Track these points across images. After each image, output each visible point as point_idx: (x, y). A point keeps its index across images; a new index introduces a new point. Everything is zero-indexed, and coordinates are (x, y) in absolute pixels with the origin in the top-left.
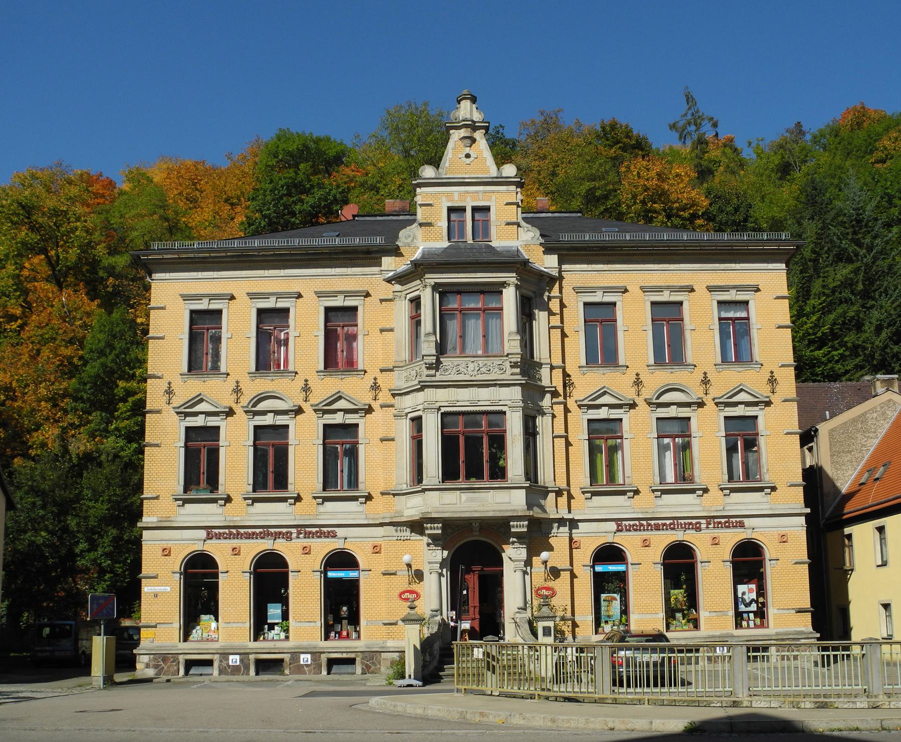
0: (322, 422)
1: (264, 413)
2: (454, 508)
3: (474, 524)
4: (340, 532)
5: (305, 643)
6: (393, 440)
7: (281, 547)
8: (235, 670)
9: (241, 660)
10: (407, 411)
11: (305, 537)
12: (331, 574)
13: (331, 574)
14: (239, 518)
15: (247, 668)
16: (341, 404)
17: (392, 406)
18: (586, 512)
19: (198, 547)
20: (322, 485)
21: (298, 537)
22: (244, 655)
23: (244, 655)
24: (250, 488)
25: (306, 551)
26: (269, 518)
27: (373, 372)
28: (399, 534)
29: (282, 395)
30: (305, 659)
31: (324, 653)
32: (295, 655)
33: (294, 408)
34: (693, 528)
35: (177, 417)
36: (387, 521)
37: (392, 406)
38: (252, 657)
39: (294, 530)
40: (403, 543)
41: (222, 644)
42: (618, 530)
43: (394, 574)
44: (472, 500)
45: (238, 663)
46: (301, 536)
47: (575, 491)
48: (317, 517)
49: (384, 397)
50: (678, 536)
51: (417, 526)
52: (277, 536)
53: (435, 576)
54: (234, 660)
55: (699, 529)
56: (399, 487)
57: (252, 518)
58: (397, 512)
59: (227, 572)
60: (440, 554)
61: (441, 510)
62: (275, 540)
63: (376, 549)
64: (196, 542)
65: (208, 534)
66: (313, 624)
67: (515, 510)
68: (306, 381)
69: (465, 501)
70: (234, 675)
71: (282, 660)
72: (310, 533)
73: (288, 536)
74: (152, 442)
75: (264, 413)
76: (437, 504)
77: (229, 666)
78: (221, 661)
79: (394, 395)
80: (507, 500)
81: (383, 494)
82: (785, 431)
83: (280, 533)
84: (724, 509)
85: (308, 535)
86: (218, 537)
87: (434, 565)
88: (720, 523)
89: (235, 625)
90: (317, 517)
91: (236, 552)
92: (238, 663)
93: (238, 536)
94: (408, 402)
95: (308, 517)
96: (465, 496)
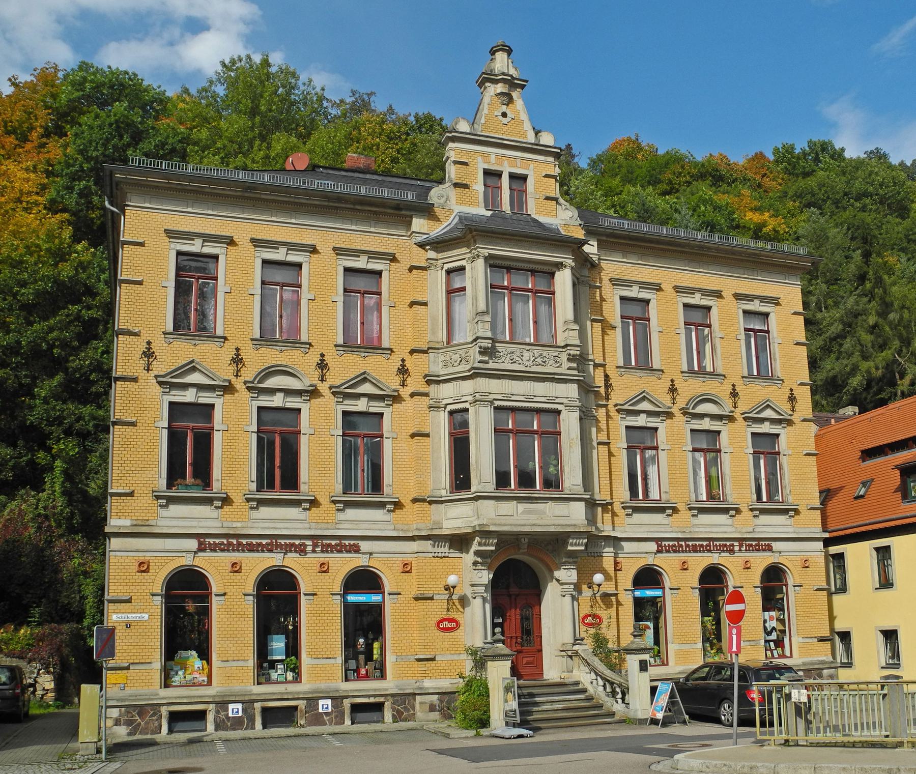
0: (341, 408)
1: (272, 391)
2: (510, 520)
3: (523, 540)
4: (364, 546)
5: (323, 685)
6: (427, 435)
7: (292, 562)
8: (237, 723)
9: (244, 710)
10: (445, 402)
11: (322, 551)
12: (352, 598)
13: (352, 598)
14: (239, 525)
15: (252, 720)
16: (367, 388)
17: (427, 395)
18: (627, 529)
19: (187, 561)
20: (341, 486)
21: (314, 551)
22: (247, 704)
23: (247, 704)
24: (254, 486)
25: (324, 569)
26: (278, 525)
27: (402, 352)
28: (436, 549)
29: (298, 371)
30: (325, 705)
31: (347, 697)
32: (312, 701)
33: (310, 388)
34: (727, 550)
35: (158, 389)
36: (423, 533)
37: (427, 395)
38: (258, 706)
39: (309, 543)
40: (440, 561)
41: (218, 689)
42: (659, 551)
43: (431, 599)
44: (529, 512)
45: (240, 714)
46: (318, 549)
47: (617, 507)
48: (337, 526)
49: (415, 383)
50: (714, 558)
51: (460, 542)
52: (288, 549)
53: (479, 601)
54: (235, 710)
55: (731, 551)
56: (437, 493)
57: (256, 525)
58: (434, 523)
59: (225, 594)
60: (486, 576)
61: (498, 522)
62: (285, 554)
63: (407, 569)
64: (184, 554)
65: (200, 544)
66: (332, 661)
67: (575, 525)
68: (322, 355)
69: (523, 513)
70: (234, 729)
71: (295, 708)
72: (329, 545)
73: (302, 550)
74: (124, 419)
75: (272, 391)
76: (492, 515)
77: (228, 718)
78: (218, 712)
79: (429, 382)
80: (565, 513)
81: (415, 501)
82: (805, 452)
83: (293, 545)
84: (754, 531)
85: (326, 549)
86: (214, 548)
87: (479, 588)
88: (751, 545)
89: (235, 664)
90: (337, 526)
91: (236, 568)
92: (240, 714)
93: (240, 548)
94: (446, 392)
95: (323, 526)
96: (522, 507)
